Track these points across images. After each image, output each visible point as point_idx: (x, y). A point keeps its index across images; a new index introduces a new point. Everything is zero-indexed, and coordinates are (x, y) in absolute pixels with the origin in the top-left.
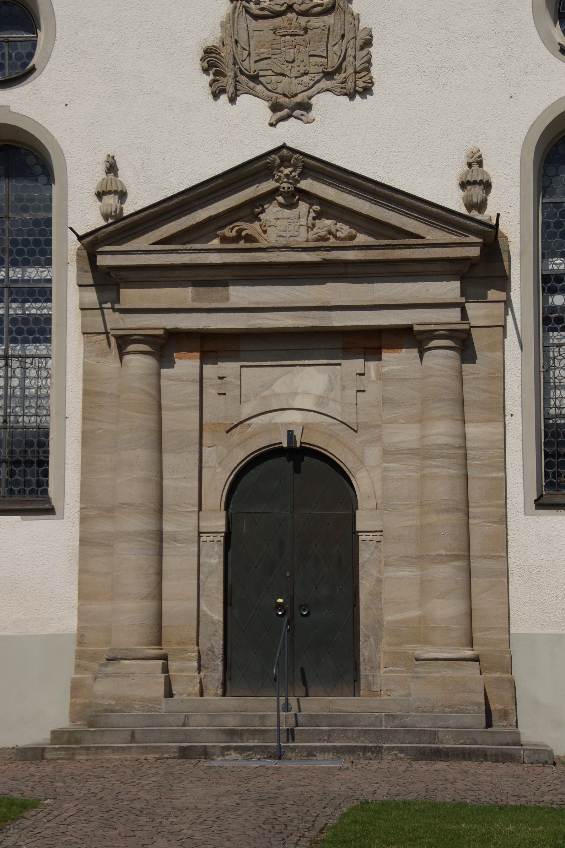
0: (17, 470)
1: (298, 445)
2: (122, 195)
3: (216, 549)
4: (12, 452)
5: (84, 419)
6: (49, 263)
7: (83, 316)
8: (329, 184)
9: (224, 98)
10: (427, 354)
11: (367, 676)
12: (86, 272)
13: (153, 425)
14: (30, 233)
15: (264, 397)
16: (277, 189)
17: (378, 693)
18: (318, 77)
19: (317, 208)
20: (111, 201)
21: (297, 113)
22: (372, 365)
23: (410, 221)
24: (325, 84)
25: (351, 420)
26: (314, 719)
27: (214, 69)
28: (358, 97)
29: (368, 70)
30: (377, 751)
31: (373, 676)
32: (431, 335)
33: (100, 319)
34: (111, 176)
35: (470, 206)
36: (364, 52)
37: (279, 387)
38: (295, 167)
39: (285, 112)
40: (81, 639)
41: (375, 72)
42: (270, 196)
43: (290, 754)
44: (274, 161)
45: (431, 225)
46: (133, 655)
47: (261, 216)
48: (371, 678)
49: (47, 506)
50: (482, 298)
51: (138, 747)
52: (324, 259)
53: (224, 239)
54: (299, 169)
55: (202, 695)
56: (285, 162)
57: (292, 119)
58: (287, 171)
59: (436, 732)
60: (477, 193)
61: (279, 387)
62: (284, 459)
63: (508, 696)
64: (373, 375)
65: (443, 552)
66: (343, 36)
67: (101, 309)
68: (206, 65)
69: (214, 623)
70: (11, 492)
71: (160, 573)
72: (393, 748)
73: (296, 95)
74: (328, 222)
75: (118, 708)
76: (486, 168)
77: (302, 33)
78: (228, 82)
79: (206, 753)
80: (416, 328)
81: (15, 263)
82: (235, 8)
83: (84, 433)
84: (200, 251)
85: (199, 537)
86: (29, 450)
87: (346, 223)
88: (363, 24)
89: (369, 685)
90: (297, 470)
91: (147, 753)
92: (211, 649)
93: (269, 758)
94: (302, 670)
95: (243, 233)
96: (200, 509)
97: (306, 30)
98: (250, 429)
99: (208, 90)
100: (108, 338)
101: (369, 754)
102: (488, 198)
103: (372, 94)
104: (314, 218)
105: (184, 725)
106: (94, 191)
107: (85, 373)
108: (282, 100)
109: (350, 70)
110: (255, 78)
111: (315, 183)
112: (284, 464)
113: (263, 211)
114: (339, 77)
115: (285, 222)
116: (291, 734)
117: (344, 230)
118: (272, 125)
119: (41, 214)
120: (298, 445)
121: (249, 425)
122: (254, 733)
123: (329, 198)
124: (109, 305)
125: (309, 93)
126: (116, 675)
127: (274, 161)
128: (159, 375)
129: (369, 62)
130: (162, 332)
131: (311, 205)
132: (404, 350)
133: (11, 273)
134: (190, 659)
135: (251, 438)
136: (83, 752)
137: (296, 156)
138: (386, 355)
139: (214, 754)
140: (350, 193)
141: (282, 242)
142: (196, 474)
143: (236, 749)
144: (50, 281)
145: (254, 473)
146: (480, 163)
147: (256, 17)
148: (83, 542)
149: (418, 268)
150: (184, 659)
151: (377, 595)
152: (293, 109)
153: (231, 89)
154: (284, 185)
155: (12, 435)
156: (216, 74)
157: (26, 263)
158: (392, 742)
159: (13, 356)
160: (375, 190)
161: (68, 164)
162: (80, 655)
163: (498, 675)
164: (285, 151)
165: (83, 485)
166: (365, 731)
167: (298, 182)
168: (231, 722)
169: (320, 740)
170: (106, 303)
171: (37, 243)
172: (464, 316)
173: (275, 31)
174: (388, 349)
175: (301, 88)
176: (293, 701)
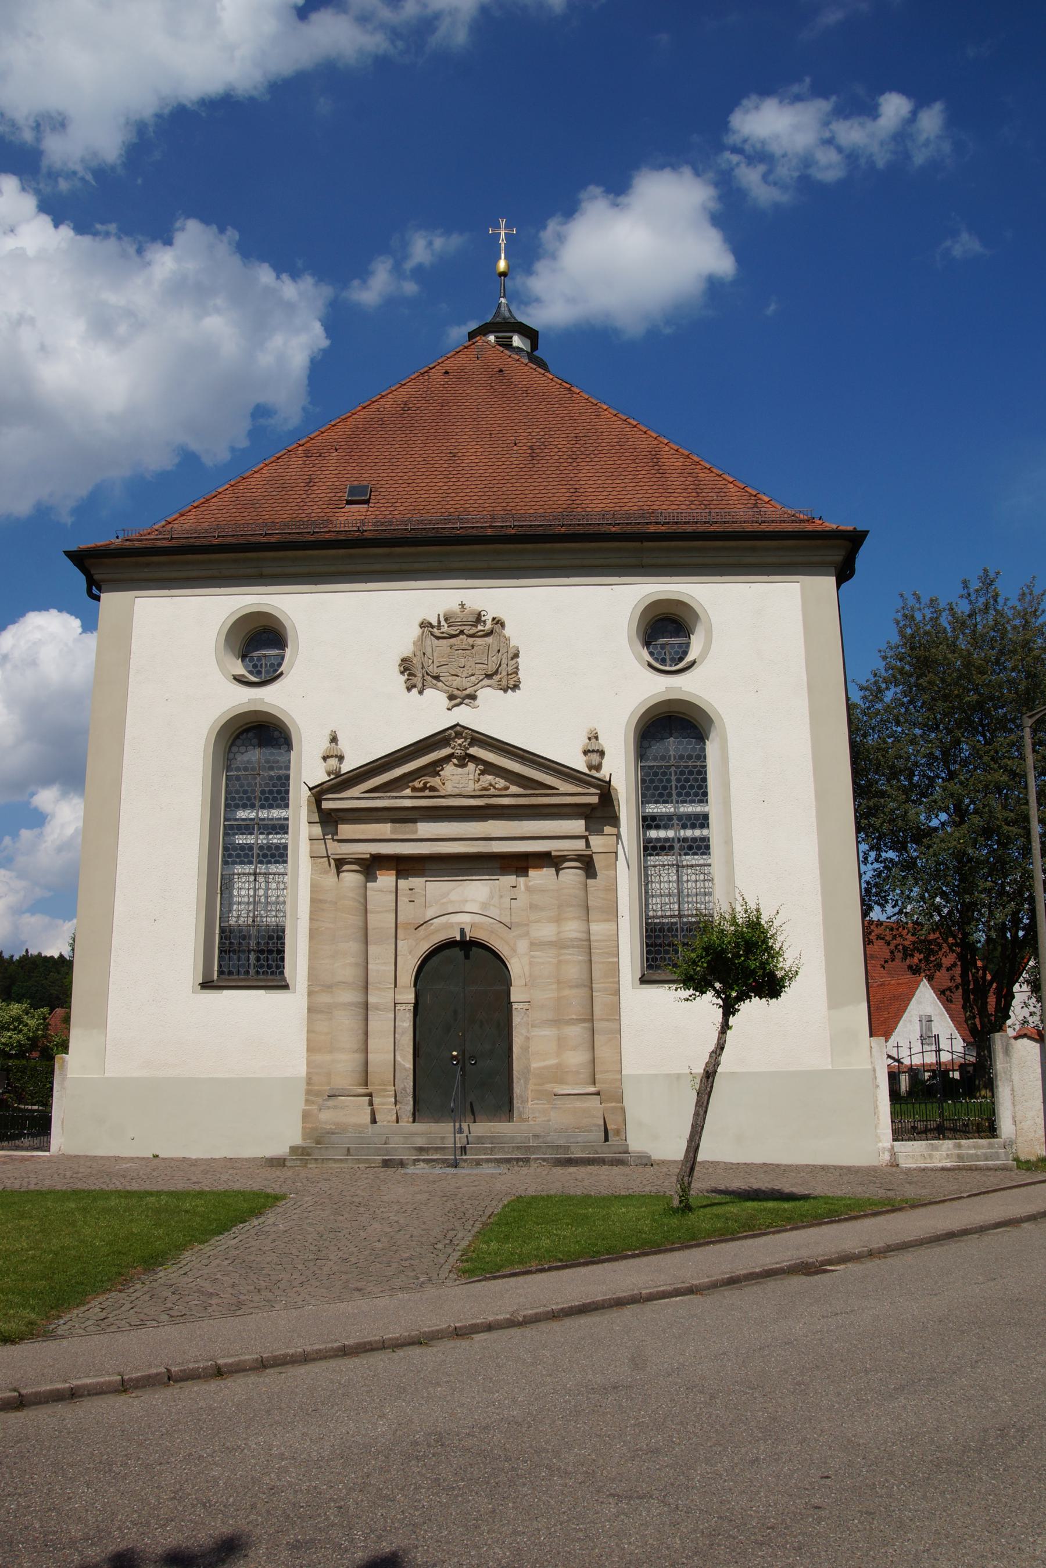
0: (262, 957)
1: (468, 939)
2: (341, 758)
4: (258, 943)
5: (311, 919)
6: (287, 806)
7: (311, 845)
8: (490, 751)
9: (415, 691)
10: (561, 872)
11: (519, 1107)
13: (361, 924)
14: (274, 786)
15: (443, 904)
17: (527, 1120)
19: (481, 767)
20: (333, 762)
21: (467, 701)
22: (522, 880)
23: (548, 777)
24: (486, 682)
25: (506, 920)
26: (480, 1139)
29: (516, 673)
30: (527, 1161)
32: (564, 858)
34: (333, 744)
35: (591, 767)
36: (514, 661)
37: (453, 896)
38: (466, 739)
39: (459, 700)
40: (309, 1081)
42: (447, 759)
43: (463, 1164)
44: (451, 734)
45: (564, 780)
46: (347, 1093)
48: (521, 1109)
49: (283, 983)
50: (600, 832)
53: (414, 789)
54: (469, 740)
55: (397, 1122)
56: (458, 735)
58: (460, 741)
59: (569, 1146)
60: (595, 758)
61: (453, 896)
62: (457, 949)
63: (620, 1119)
64: (523, 887)
65: (575, 1017)
66: (499, 651)
67: (324, 839)
68: (402, 669)
69: (406, 1069)
70: (258, 973)
71: (366, 1033)
72: (538, 1159)
73: (466, 689)
76: (601, 741)
77: (470, 648)
78: (418, 680)
79: (402, 1164)
80: (553, 853)
81: (263, 807)
82: (423, 632)
83: (310, 930)
84: (396, 798)
85: (395, 1007)
86: (271, 942)
87: (502, 778)
88: (512, 644)
89: (520, 1114)
90: (467, 957)
92: (404, 1089)
93: (448, 1167)
94: (471, 1104)
95: (428, 785)
96: (395, 986)
97: (473, 647)
98: (432, 927)
99: (404, 686)
100: (329, 860)
101: (521, 1163)
102: (604, 762)
103: (519, 689)
104: (479, 775)
105: (385, 1144)
106: (321, 755)
107: (312, 886)
108: (456, 692)
109: (504, 673)
110: (437, 678)
112: (457, 953)
113: (442, 769)
114: (496, 678)
115: (458, 777)
116: (464, 1150)
117: (501, 783)
118: (448, 709)
120: (468, 939)
121: (432, 924)
122: (437, 1149)
123: (490, 760)
124: (330, 836)
125: (475, 688)
126: (335, 1107)
127: (451, 734)
128: (366, 887)
129: (517, 668)
130: (368, 856)
131: (477, 765)
133: (260, 814)
134: (389, 1096)
136: (313, 1161)
138: (532, 873)
139: (407, 1164)
141: (456, 791)
142: (393, 961)
143: (424, 1160)
144: (287, 819)
145: (435, 959)
146: (597, 738)
147: (438, 638)
148: (311, 1010)
149: (555, 810)
150: (384, 1096)
151: (526, 1049)
152: (464, 699)
153: (420, 685)
154: (457, 751)
155: (259, 931)
156: (409, 675)
157: (271, 807)
158: (537, 1154)
159: (260, 874)
162: (308, 1092)
163: (613, 1104)
165: (311, 968)
166: (518, 1147)
167: (468, 749)
168: (420, 1142)
169: (485, 1154)
171: (279, 792)
172: (588, 845)
173: (451, 647)
176: (465, 1126)
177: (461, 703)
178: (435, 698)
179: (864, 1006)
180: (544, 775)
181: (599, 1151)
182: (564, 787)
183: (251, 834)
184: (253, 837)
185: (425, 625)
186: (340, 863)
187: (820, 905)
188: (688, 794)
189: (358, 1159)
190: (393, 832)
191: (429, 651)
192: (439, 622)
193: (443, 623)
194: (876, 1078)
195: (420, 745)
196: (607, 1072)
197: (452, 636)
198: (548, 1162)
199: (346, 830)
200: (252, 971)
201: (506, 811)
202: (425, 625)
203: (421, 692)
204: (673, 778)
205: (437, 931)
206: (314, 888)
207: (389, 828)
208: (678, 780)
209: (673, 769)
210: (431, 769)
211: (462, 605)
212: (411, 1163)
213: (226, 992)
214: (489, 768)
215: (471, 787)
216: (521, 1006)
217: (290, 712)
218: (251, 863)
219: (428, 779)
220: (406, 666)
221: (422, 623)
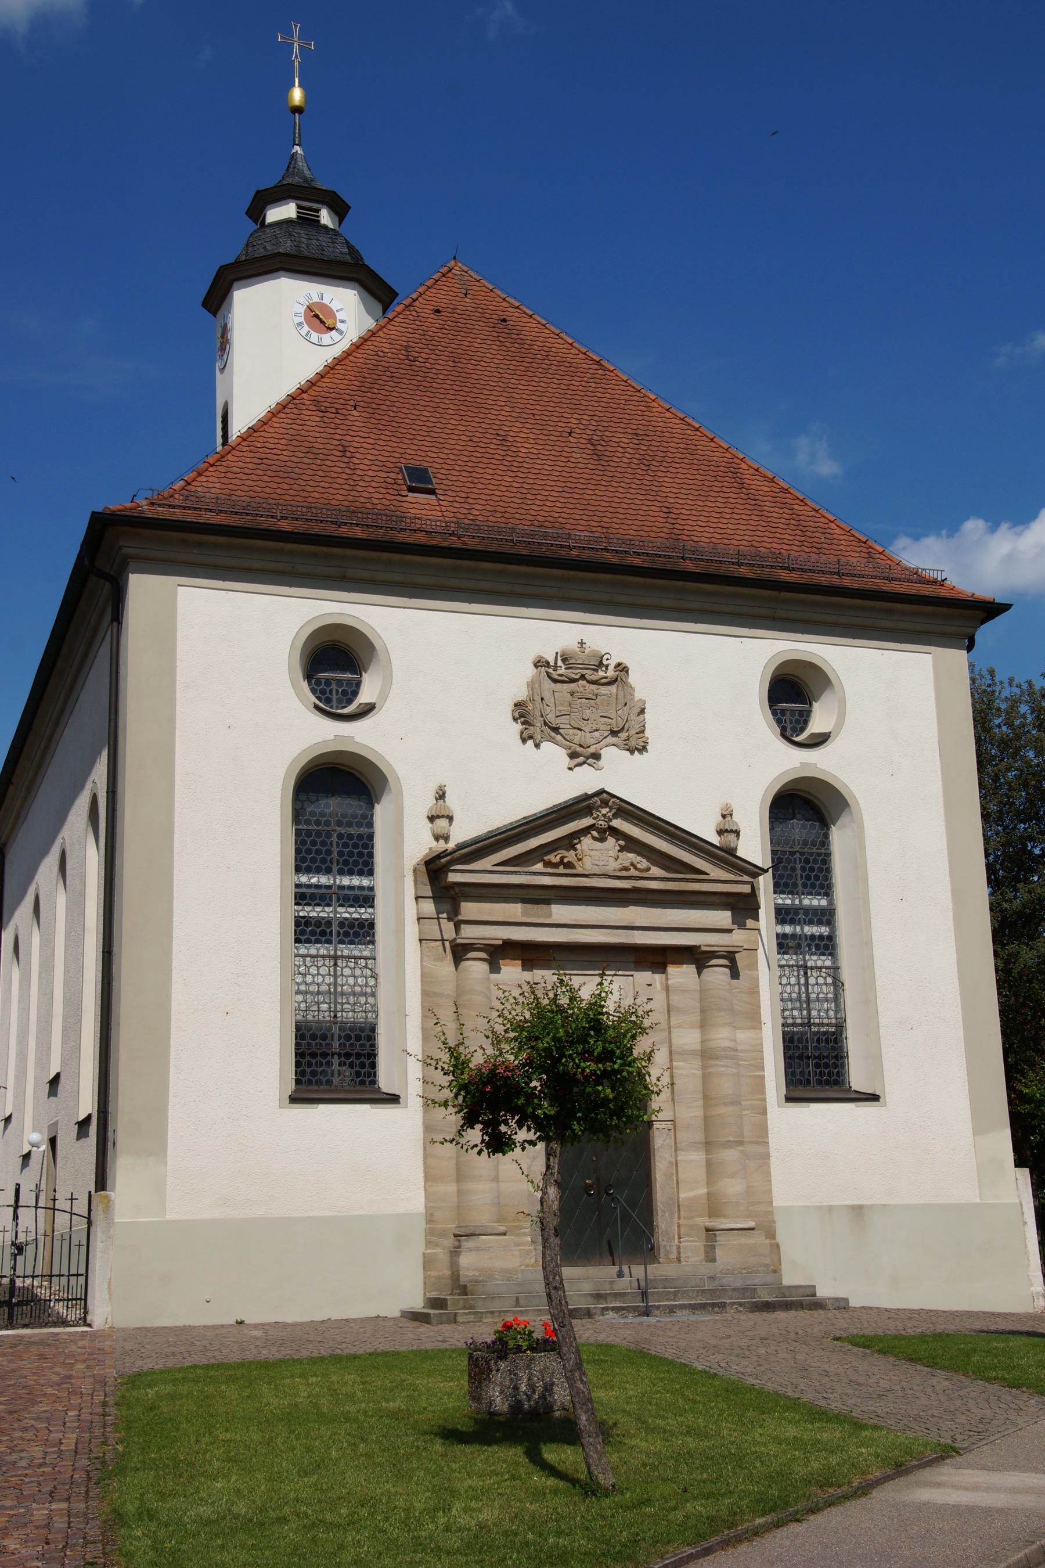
6: (371, 873)
8: (636, 825)
9: (530, 743)
11: (665, 1246)
12: (425, 885)
14: (356, 846)
16: (594, 824)
18: (606, 734)
19: (622, 843)
21: (590, 761)
24: (611, 740)
27: (523, 719)
28: (636, 752)
29: (643, 732)
30: (723, 1306)
31: (670, 1246)
32: (713, 955)
33: (437, 927)
34: (441, 802)
38: (611, 808)
40: (430, 1218)
41: (647, 733)
44: (595, 803)
45: (714, 864)
48: (668, 1248)
51: (534, 1310)
52: (634, 887)
56: (605, 803)
59: (756, 1289)
67: (438, 918)
72: (734, 1303)
73: (589, 747)
74: (631, 855)
75: (481, 1278)
80: (704, 949)
81: (341, 872)
87: (644, 857)
91: (542, 1315)
93: (639, 1315)
95: (566, 860)
100: (444, 945)
103: (647, 752)
104: (619, 851)
108: (579, 749)
110: (556, 730)
111: (624, 823)
114: (624, 735)
115: (598, 853)
117: (643, 863)
118: (570, 769)
119: (363, 830)
123: (635, 836)
124: (445, 915)
126: (478, 1249)
127: (595, 803)
130: (501, 942)
131: (617, 840)
132: (685, 966)
134: (525, 1234)
136: (489, 1315)
137: (613, 800)
138: (671, 969)
139: (595, 1314)
140: (651, 833)
144: (371, 889)
147: (555, 681)
149: (702, 898)
150: (519, 1235)
152: (587, 758)
154: (600, 822)
157: (351, 873)
160: (675, 833)
161: (404, 789)
162: (430, 1232)
167: (610, 820)
169: (668, 1300)
170: (442, 913)
171: (360, 855)
173: (572, 694)
174: (672, 964)
175: (593, 741)
176: (625, 1269)
177: (584, 763)
178: (554, 753)
179: (1008, 1132)
180: (694, 858)
181: (787, 1294)
182: (715, 872)
183: (329, 905)
184: (331, 909)
185: (540, 663)
186: (460, 952)
187: (961, 1020)
188: (813, 886)
189: (540, 1310)
190: (525, 913)
191: (547, 695)
192: (556, 663)
193: (560, 663)
194: (1023, 1214)
195: (563, 812)
196: (759, 1203)
197: (572, 681)
199: (470, 909)
201: (650, 896)
202: (540, 663)
203: (537, 746)
204: (798, 866)
206: (426, 978)
207: (520, 910)
208: (803, 869)
209: (797, 855)
210: (567, 842)
212: (598, 1312)
213: (322, 1107)
214: (631, 844)
215: (612, 866)
216: (663, 1125)
217: (387, 757)
218: (329, 942)
219: (564, 853)
220: (521, 712)
221: (539, 662)
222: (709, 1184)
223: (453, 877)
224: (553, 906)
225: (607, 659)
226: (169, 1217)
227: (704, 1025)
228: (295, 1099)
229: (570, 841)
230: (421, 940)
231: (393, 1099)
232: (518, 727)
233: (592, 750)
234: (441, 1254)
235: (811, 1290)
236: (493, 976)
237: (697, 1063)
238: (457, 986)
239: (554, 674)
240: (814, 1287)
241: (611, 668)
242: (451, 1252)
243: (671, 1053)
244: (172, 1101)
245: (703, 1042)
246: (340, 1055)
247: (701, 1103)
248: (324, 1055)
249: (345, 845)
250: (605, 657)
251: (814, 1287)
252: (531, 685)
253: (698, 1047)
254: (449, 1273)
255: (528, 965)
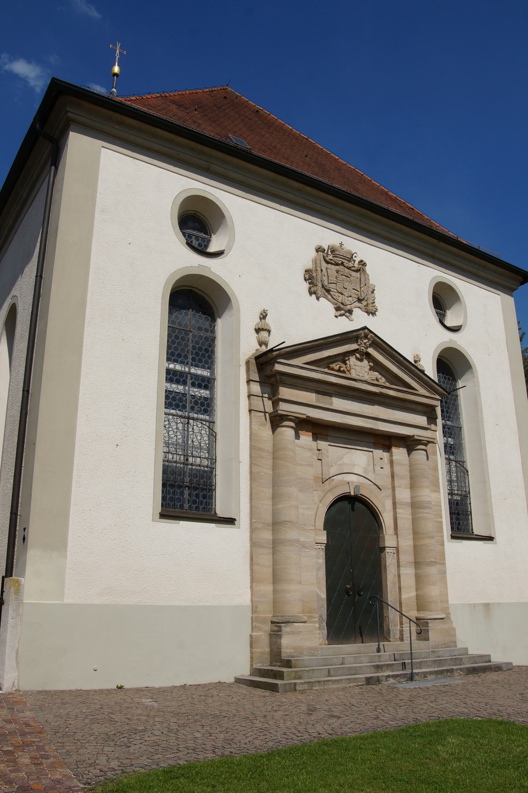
3: (322, 554)
9: (314, 296)
12: (255, 373)
15: (340, 464)
16: (358, 349)
19: (371, 364)
21: (347, 314)
24: (357, 304)
27: (310, 281)
28: (371, 315)
29: (374, 303)
31: (396, 630)
33: (262, 403)
37: (346, 460)
39: (343, 312)
40: (254, 609)
42: (352, 353)
44: (361, 334)
45: (422, 386)
47: (348, 362)
51: (345, 679)
52: (381, 392)
54: (370, 342)
56: (366, 337)
57: (344, 316)
61: (346, 460)
67: (262, 397)
74: (376, 373)
75: (295, 654)
80: (416, 437)
87: (383, 376)
91: (350, 683)
98: (333, 483)
100: (265, 415)
103: (376, 316)
105: (342, 664)
108: (342, 306)
110: (328, 291)
111: (374, 351)
112: (345, 504)
114: (364, 303)
118: (336, 317)
119: (209, 334)
121: (333, 480)
124: (266, 395)
126: (293, 633)
127: (361, 334)
131: (369, 362)
132: (401, 448)
134: (314, 622)
135: (334, 488)
136: (317, 684)
137: (372, 334)
138: (394, 450)
139: (382, 681)
147: (327, 262)
149: (413, 406)
154: (362, 348)
160: (402, 362)
161: (241, 308)
164: (366, 331)
166: (435, 661)
167: (367, 348)
170: (265, 394)
171: (207, 351)
173: (337, 272)
174: (395, 447)
177: (343, 315)
180: (411, 380)
181: (477, 661)
182: (422, 391)
185: (319, 250)
189: (349, 679)
193: (329, 253)
195: (344, 337)
198: (463, 672)
199: (285, 392)
200: (186, 506)
201: (387, 401)
202: (319, 250)
203: (318, 299)
205: (336, 487)
207: (314, 398)
210: (341, 358)
211: (341, 244)
212: (384, 679)
213: (182, 523)
214: (377, 366)
217: (231, 285)
221: (319, 248)
222: (417, 589)
223: (278, 367)
224: (333, 398)
225: (355, 257)
226: (67, 601)
227: (413, 486)
228: (163, 516)
229: (343, 357)
230: (250, 411)
231: (230, 521)
232: (306, 285)
233: (348, 307)
234: (263, 636)
235: (487, 658)
236: (296, 440)
237: (409, 510)
238: (274, 445)
239: (327, 259)
240: (490, 655)
241: (357, 262)
242: (271, 635)
243: (394, 504)
244: (73, 509)
245: (412, 497)
246: (189, 488)
247: (411, 537)
248: (180, 487)
249: (197, 343)
250: (355, 255)
251: (490, 655)
252: (315, 261)
253: (409, 501)
254: (268, 650)
255: (316, 437)
